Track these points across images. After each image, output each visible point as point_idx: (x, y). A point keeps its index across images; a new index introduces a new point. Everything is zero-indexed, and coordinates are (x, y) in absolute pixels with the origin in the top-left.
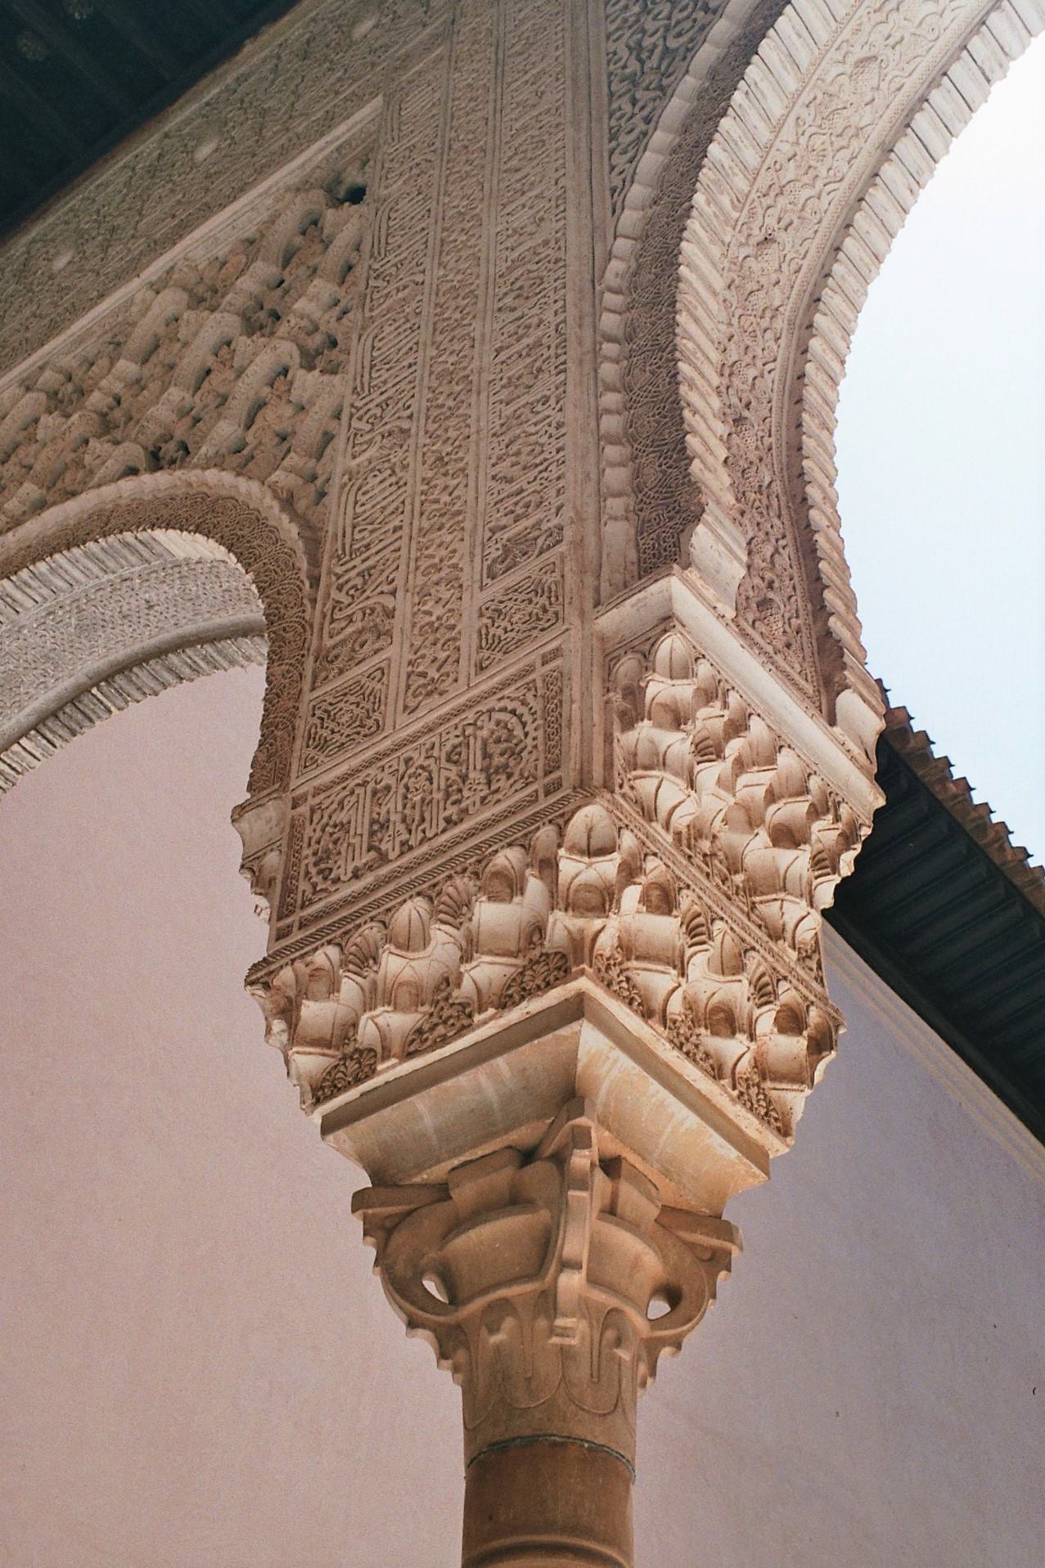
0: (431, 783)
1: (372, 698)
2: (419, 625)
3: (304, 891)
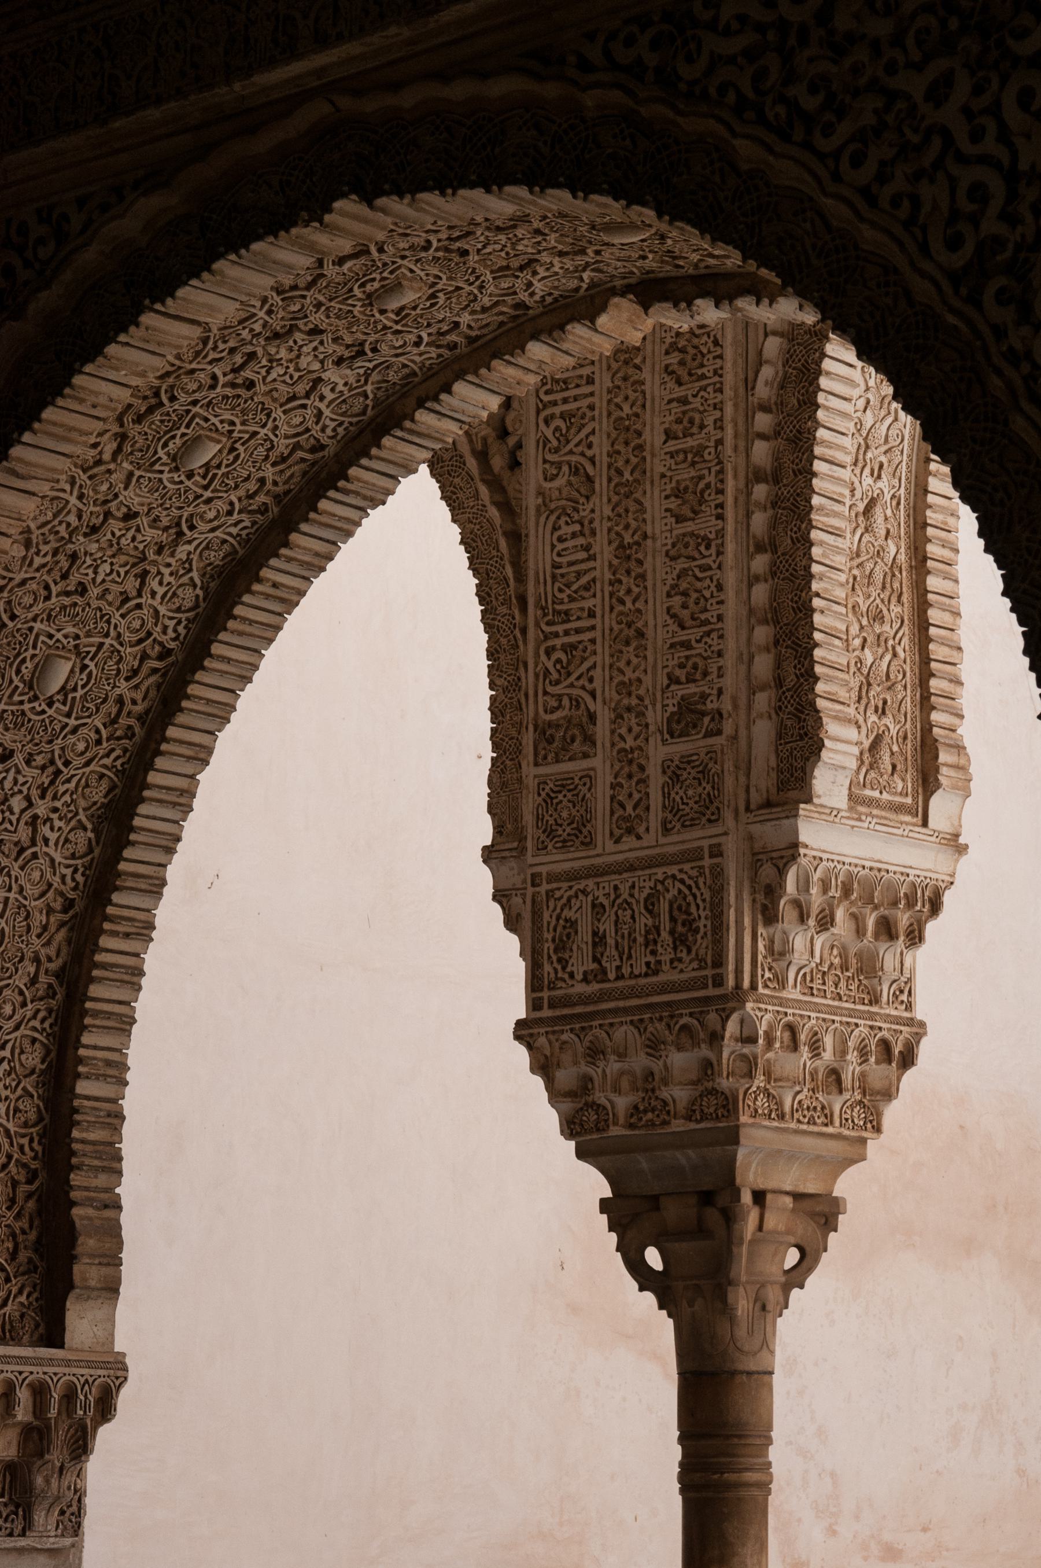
0: (635, 921)
2: (617, 748)
3: (549, 973)
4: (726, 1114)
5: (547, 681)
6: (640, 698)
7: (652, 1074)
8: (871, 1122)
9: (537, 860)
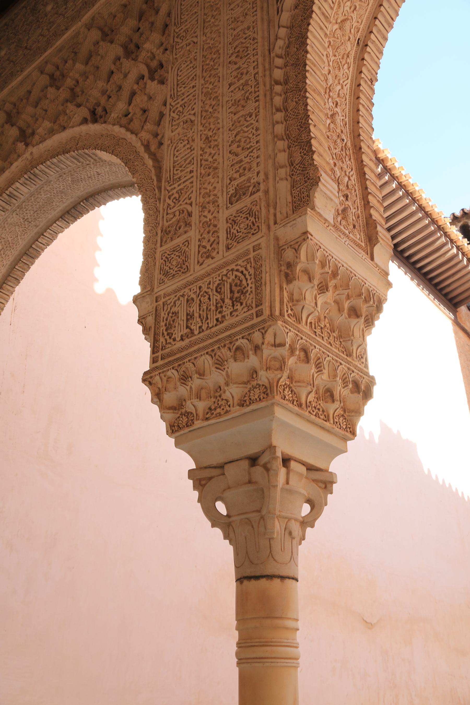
0: (210, 301)
1: (184, 254)
2: (202, 222)
3: (162, 342)
4: (265, 396)
5: (169, 208)
6: (215, 195)
7: (220, 387)
8: (350, 428)
9: (159, 289)
